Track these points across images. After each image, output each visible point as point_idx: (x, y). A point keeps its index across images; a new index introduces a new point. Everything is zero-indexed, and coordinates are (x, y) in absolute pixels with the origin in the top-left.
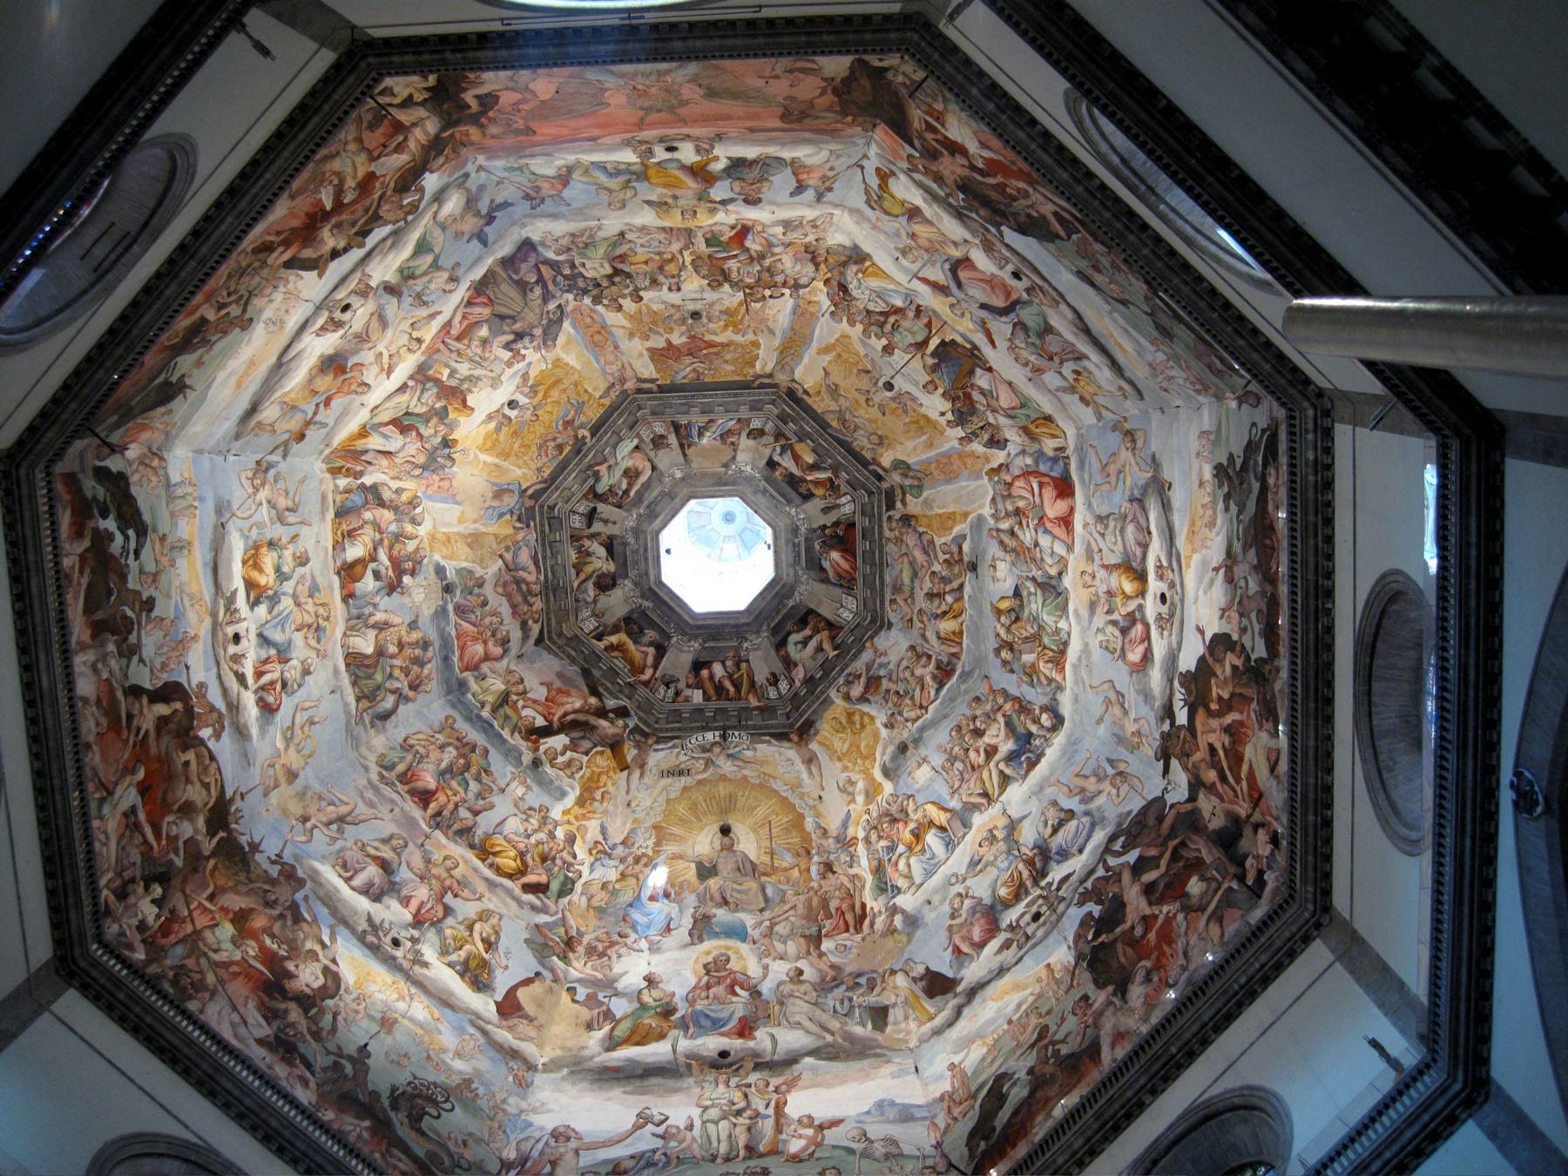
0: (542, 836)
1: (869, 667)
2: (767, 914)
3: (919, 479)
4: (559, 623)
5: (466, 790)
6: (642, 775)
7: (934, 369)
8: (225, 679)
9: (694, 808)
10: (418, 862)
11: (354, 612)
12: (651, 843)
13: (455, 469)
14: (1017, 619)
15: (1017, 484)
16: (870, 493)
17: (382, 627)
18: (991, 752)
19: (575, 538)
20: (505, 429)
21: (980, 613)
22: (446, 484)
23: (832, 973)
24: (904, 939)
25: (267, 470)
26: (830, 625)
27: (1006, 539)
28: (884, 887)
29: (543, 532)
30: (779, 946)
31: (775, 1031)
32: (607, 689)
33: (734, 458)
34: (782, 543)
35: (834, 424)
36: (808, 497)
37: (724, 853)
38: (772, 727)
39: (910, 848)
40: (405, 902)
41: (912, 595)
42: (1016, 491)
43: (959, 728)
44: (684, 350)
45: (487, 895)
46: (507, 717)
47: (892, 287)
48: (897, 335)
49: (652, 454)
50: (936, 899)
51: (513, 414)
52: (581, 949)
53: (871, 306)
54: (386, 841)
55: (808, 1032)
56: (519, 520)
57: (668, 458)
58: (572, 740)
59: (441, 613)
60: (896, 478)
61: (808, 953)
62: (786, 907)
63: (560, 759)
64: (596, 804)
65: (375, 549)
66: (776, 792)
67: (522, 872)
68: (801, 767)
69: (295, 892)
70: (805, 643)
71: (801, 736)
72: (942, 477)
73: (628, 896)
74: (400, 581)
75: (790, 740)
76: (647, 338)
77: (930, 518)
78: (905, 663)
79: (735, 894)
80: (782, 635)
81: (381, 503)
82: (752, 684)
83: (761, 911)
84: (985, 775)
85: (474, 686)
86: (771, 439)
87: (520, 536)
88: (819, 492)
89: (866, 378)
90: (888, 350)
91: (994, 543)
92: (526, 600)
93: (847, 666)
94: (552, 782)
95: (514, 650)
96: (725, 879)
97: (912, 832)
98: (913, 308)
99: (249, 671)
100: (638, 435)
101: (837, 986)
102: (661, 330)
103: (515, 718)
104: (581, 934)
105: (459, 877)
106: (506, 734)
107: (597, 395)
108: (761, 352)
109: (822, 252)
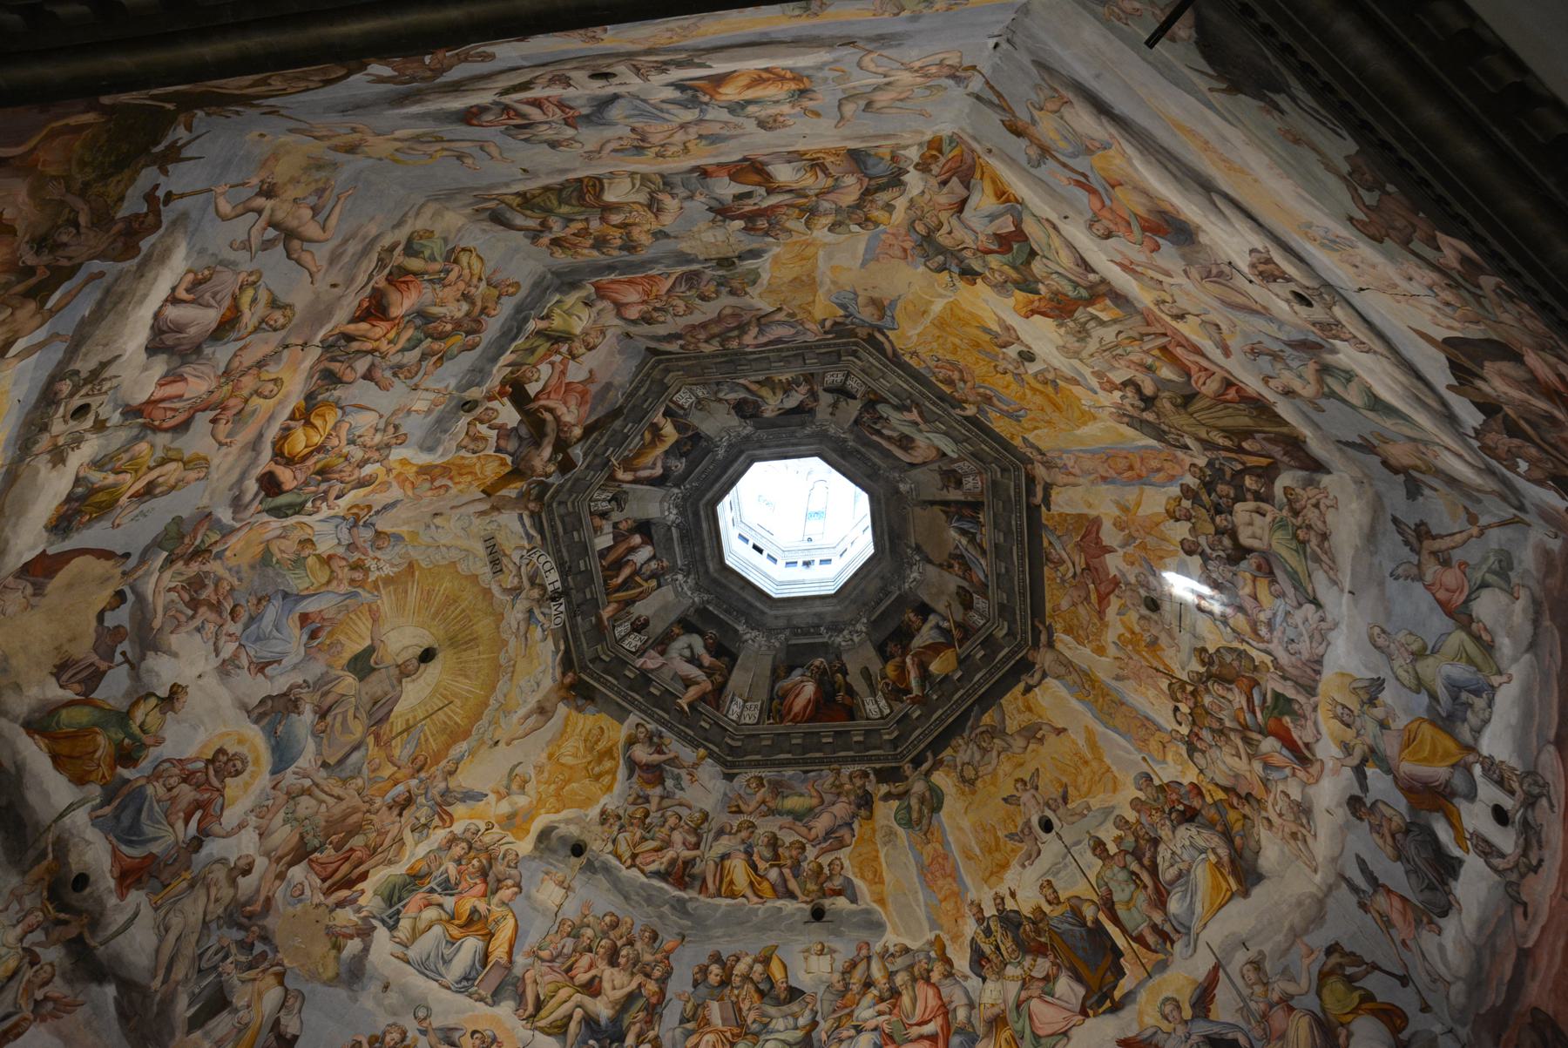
0: (357, 454)
1: (674, 761)
2: (323, 773)
3: (919, 821)
4: (682, 369)
5: (403, 350)
6: (482, 513)
7: (1076, 913)
8: (513, 74)
9: (451, 600)
10: (249, 358)
11: (677, 180)
12: (388, 570)
13: (922, 269)
14: (762, 994)
15: (931, 992)
16: (895, 743)
17: (654, 206)
18: (592, 988)
19: (809, 378)
20: (987, 337)
21: (762, 928)
22: (899, 253)
23: (257, 907)
24: (330, 973)
25: (953, 77)
26: (719, 689)
27: (858, 976)
28: (394, 896)
29: (819, 347)
30: (281, 815)
31: (146, 910)
32: (596, 441)
33: (930, 562)
34: (818, 608)
35: (986, 719)
36: (885, 657)
37: (397, 671)
38: (578, 647)
39: (452, 917)
40: (172, 377)
41: (772, 812)
42: (921, 987)
43: (615, 925)
44: (1094, 562)
45: (234, 449)
46: (532, 351)
47: (1198, 909)
48: (1122, 876)
49: (935, 466)
50: (393, 998)
51: (1012, 352)
52: (195, 567)
53: (1163, 853)
54: (274, 304)
55: (157, 951)
56: (836, 324)
57: (928, 482)
58: (515, 429)
59: (684, 258)
60: (919, 787)
61: (280, 858)
62: (337, 791)
63: (483, 429)
64: (427, 485)
65: (791, 191)
66: (494, 688)
67: (290, 462)
68: (532, 702)
69: (102, 256)
70: (693, 660)
71: (572, 687)
72: (927, 860)
73: (297, 583)
74: (733, 218)
75: (564, 674)
76: (1119, 525)
77: (872, 841)
78: (684, 812)
79: (339, 719)
80: (700, 625)
81: (867, 193)
82: (631, 602)
83: (325, 765)
84: (564, 993)
85: (572, 298)
86: (959, 617)
87: (809, 325)
88: (890, 670)
89: (1056, 793)
90: (1099, 847)
91: (852, 953)
92: (713, 336)
93: (670, 729)
94: (445, 431)
95: (633, 329)
96: (358, 695)
97: (474, 911)
98: (1167, 928)
99: (536, 93)
100: (960, 459)
101: (241, 927)
102: (1130, 549)
103: (531, 360)
104: (219, 556)
105: (249, 408)
106: (507, 357)
107: (1030, 437)
108: (1088, 651)
109: (1247, 810)
